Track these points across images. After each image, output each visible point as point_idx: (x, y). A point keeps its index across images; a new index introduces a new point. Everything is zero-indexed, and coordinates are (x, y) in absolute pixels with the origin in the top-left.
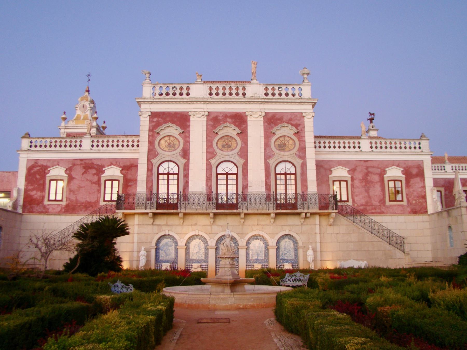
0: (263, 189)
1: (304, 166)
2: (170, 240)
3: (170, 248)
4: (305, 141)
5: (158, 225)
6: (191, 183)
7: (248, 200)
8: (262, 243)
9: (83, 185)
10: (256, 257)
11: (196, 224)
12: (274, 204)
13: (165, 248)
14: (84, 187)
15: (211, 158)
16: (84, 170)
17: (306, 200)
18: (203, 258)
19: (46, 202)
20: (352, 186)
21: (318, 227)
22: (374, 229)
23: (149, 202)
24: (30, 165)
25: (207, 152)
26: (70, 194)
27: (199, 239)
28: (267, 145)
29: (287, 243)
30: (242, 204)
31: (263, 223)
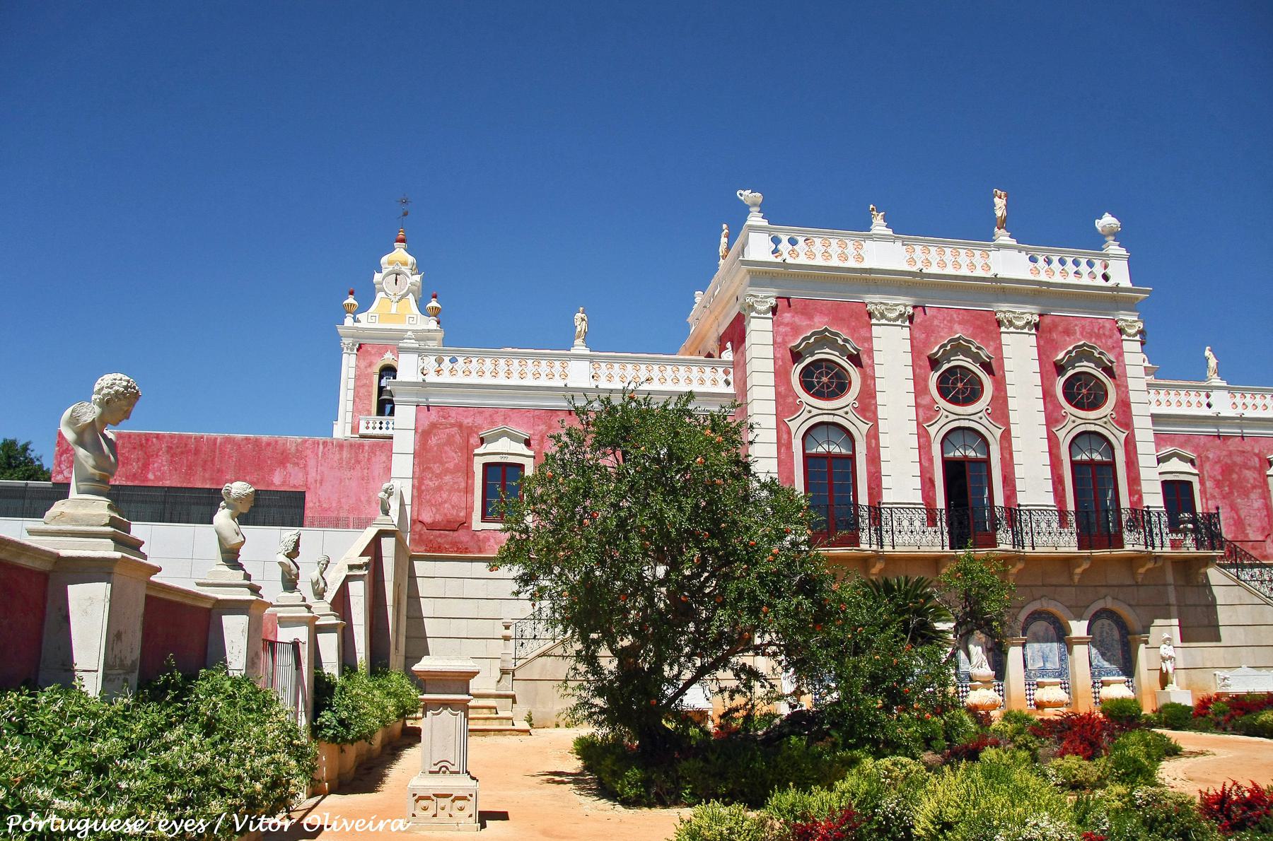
0: (1050, 500)
1: (1130, 444)
6: (885, 482)
15: (928, 419)
20: (1203, 492)
21: (1171, 589)
24: (425, 424)
25: (917, 406)
28: (1047, 395)
31: (1054, 581)
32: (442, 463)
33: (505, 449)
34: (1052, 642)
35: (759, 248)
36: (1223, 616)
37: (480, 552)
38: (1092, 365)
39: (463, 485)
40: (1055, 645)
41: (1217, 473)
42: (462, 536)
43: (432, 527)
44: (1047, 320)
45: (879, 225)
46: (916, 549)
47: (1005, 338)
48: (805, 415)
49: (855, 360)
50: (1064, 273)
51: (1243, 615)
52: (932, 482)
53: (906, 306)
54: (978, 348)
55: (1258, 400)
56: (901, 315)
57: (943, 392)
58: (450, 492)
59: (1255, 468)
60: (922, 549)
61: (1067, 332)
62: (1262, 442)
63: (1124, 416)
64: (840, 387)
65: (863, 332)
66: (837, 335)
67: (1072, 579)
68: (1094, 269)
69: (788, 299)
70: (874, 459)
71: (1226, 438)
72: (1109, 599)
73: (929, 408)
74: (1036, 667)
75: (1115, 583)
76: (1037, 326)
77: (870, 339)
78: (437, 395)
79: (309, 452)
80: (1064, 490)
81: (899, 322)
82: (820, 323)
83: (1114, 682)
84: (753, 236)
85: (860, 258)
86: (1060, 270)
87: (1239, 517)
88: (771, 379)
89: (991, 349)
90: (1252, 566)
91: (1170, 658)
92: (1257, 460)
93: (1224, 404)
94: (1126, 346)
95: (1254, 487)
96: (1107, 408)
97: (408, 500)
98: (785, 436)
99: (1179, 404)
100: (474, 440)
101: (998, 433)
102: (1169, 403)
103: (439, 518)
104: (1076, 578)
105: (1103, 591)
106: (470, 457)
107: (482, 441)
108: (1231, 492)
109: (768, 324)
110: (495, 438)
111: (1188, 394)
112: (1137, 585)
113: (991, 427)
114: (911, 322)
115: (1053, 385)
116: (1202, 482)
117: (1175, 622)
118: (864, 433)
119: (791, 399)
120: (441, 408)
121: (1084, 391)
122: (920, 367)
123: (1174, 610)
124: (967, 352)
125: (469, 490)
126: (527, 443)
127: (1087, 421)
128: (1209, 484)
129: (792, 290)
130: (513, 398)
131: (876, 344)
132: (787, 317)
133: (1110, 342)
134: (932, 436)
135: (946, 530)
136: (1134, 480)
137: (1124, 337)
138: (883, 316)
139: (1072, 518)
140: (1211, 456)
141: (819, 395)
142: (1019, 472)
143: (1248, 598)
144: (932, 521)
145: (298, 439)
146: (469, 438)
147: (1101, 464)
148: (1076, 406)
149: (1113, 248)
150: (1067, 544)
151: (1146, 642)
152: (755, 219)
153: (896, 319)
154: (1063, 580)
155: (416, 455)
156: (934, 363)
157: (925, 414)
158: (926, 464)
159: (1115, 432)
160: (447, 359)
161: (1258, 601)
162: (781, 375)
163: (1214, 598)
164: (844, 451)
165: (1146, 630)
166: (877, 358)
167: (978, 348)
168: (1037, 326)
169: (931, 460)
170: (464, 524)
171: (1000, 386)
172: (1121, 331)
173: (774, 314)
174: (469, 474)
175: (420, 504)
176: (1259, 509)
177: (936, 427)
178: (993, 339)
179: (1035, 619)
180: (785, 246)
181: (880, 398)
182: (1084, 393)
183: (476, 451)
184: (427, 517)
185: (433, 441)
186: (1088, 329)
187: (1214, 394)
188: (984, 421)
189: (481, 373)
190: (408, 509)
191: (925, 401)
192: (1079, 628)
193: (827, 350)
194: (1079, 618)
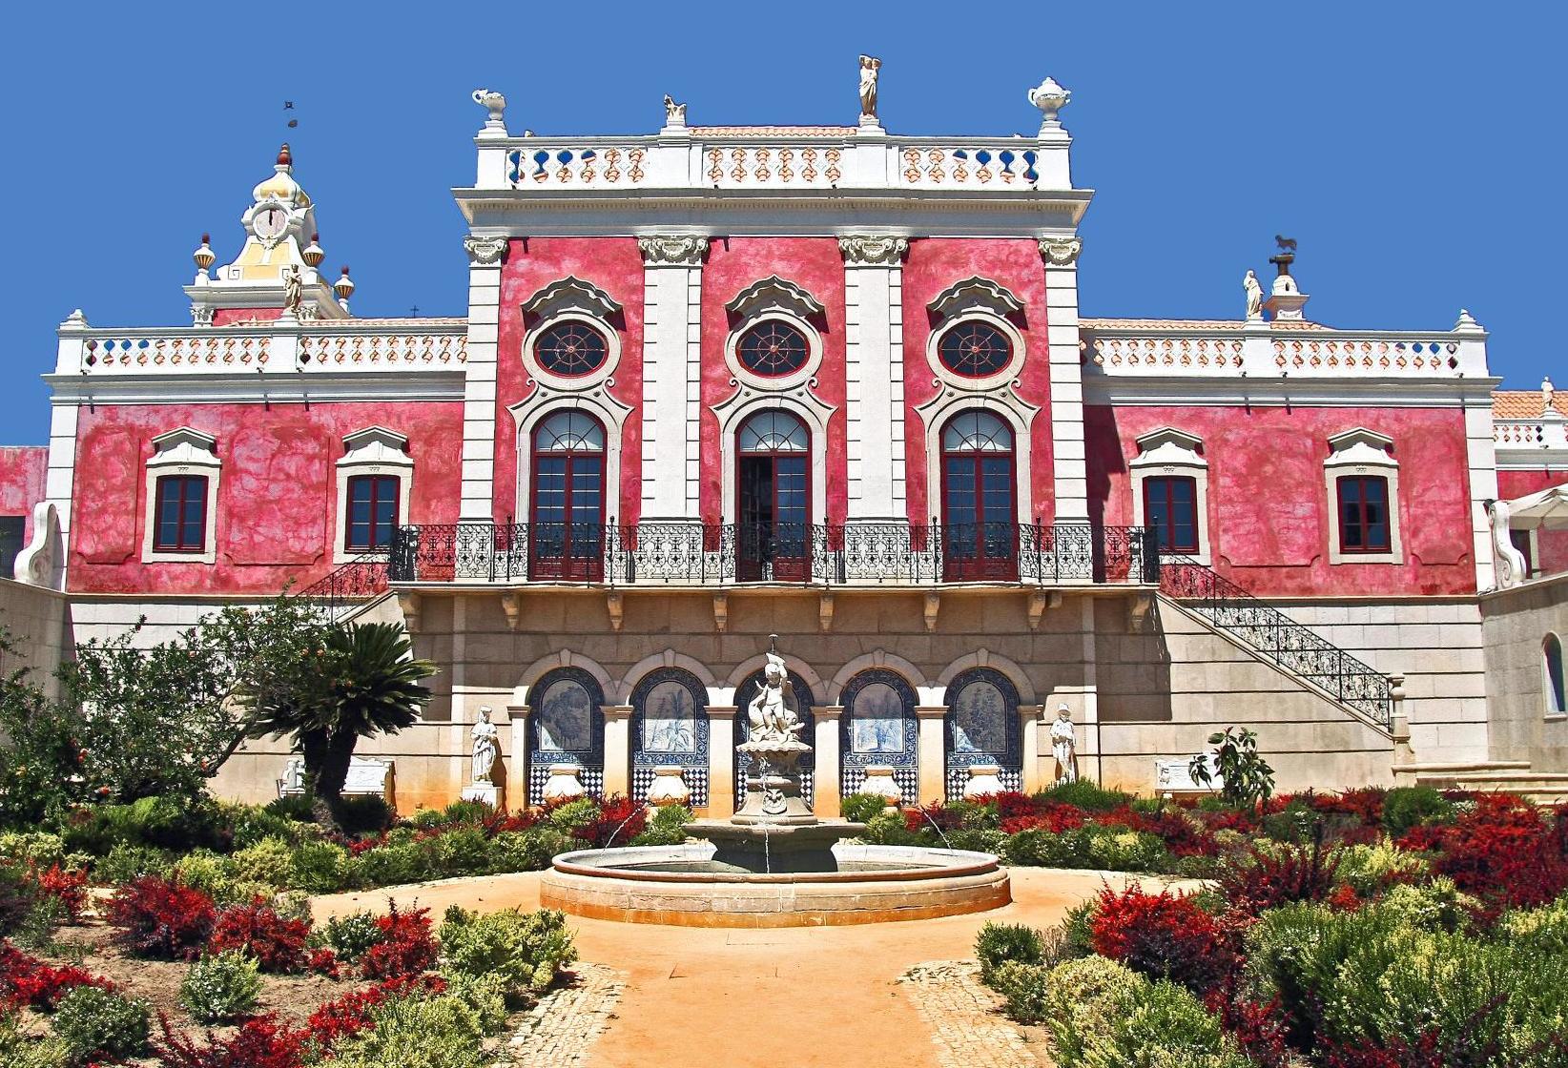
0: (900, 510)
1: (1042, 427)
2: (576, 685)
3: (577, 712)
4: (1047, 340)
5: (536, 633)
6: (647, 489)
7: (848, 547)
8: (894, 694)
9: (275, 491)
10: (875, 745)
11: (665, 631)
12: (936, 561)
13: (560, 711)
14: (279, 501)
15: (719, 399)
16: (277, 442)
17: (1048, 549)
18: (691, 748)
19: (148, 555)
21: (1089, 640)
22: (1286, 650)
23: (504, 554)
26: (229, 526)
27: (678, 680)
29: (984, 695)
30: (826, 560)
31: (896, 627)
32: (107, 478)
33: (186, 457)
34: (893, 717)
35: (492, 172)
36: (1179, 678)
37: (150, 590)
38: (991, 310)
39: (132, 505)
40: (900, 721)
41: (1239, 462)
42: (130, 570)
43: (94, 560)
44: (924, 246)
45: (675, 125)
46: (876, 582)
47: (851, 277)
48: (538, 400)
49: (818, 320)
50: (961, 175)
51: (1215, 677)
52: (717, 487)
53: (895, 239)
54: (802, 293)
55: (1358, 351)
56: (888, 253)
57: (747, 359)
58: (115, 514)
59: (1305, 456)
60: (671, 582)
61: (955, 263)
62: (1322, 415)
63: (1037, 386)
64: (1000, 356)
65: (633, 280)
66: (588, 286)
67: (820, 624)
68: (988, 166)
69: (525, 240)
70: (633, 458)
71: (1263, 409)
72: (983, 654)
73: (722, 382)
74: (865, 749)
75: (995, 630)
76: (904, 256)
77: (641, 289)
78: (318, 389)
79: (29, 466)
80: (925, 495)
81: (885, 263)
82: (570, 268)
83: (877, 774)
84: (484, 155)
85: (833, 173)
86: (947, 172)
87: (1270, 530)
88: (491, 352)
89: (827, 293)
90: (1239, 605)
91: (1063, 740)
92: (1309, 442)
93: (1260, 360)
94: (1052, 278)
95: (1300, 485)
96: (1009, 374)
97: (65, 526)
98: (507, 430)
99: (1334, 362)
100: (148, 447)
101: (825, 415)
102: (1186, 360)
103: (101, 548)
104: (930, 624)
105: (978, 641)
106: (331, 470)
107: (157, 448)
108: (1259, 493)
109: (494, 277)
110: (172, 444)
111: (1298, 347)
112: (1033, 634)
113: (816, 407)
114: (705, 261)
115: (922, 341)
116: (1212, 479)
117: (1094, 688)
118: (620, 422)
119: (519, 379)
120: (111, 409)
121: (974, 349)
122: (715, 325)
123: (1090, 670)
124: (786, 301)
125: (139, 511)
126: (213, 449)
127: (972, 394)
128: (1224, 481)
129: (529, 224)
130: (140, 391)
131: (649, 296)
132: (523, 264)
133: (1025, 274)
134: (723, 423)
135: (940, 554)
136: (1044, 477)
137: (1049, 265)
138: (661, 255)
139: (934, 537)
140: (1231, 437)
141: (561, 371)
142: (853, 470)
143: (1225, 651)
144: (712, 541)
145: (17, 449)
146: (141, 443)
147: (994, 456)
148: (959, 372)
149: (1051, 131)
150: (926, 574)
151: (1040, 716)
152: (494, 131)
153: (681, 258)
154: (911, 625)
155: (77, 468)
156: (735, 319)
157: (713, 389)
158: (709, 461)
159: (1019, 408)
160: (118, 344)
161: (1241, 655)
162: (507, 346)
163: (1167, 655)
164: (1000, 448)
165: (1040, 699)
166: (650, 314)
167: (802, 293)
168: (904, 256)
169: (718, 457)
170: (131, 556)
171: (837, 345)
172: (1045, 257)
173: (504, 262)
174: (140, 491)
175: (80, 531)
176: (1304, 518)
177: (935, 408)
178: (833, 279)
179: (869, 682)
180: (528, 165)
181: (648, 371)
182: (975, 351)
183: (150, 462)
184: (88, 548)
185: (97, 450)
186: (991, 255)
187: (1249, 344)
188: (806, 399)
189: (194, 359)
190: (65, 538)
191: (718, 372)
192: (932, 697)
193: (778, 308)
194: (932, 681)
